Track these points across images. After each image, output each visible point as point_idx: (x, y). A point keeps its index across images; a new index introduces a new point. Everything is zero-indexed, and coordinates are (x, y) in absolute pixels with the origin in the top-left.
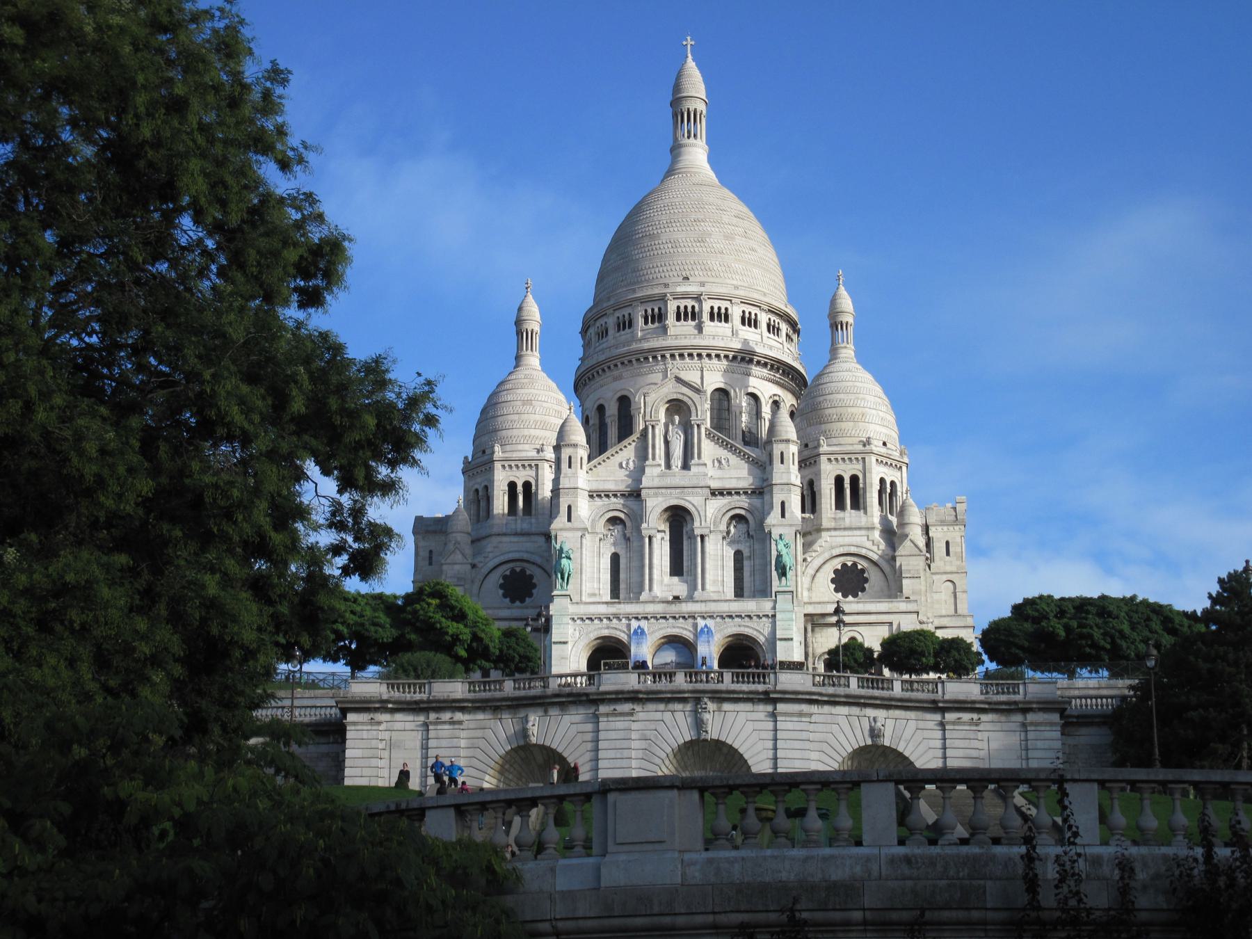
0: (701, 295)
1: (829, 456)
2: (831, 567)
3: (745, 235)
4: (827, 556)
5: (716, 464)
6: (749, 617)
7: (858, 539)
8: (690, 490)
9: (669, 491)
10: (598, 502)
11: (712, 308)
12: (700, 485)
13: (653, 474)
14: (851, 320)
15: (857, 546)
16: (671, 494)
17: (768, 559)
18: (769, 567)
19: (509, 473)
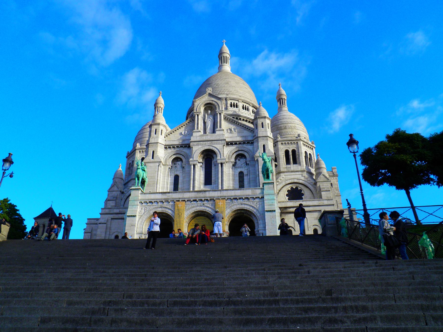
0: (227, 98)
1: (282, 142)
2: (286, 189)
3: (243, 84)
4: (284, 184)
5: (229, 131)
6: (247, 198)
7: (298, 176)
8: (215, 142)
9: (204, 143)
10: (169, 151)
11: (231, 103)
12: (221, 139)
13: (197, 136)
14: (286, 98)
15: (298, 179)
16: (205, 144)
17: (257, 173)
18: (258, 178)
19: (142, 154)
